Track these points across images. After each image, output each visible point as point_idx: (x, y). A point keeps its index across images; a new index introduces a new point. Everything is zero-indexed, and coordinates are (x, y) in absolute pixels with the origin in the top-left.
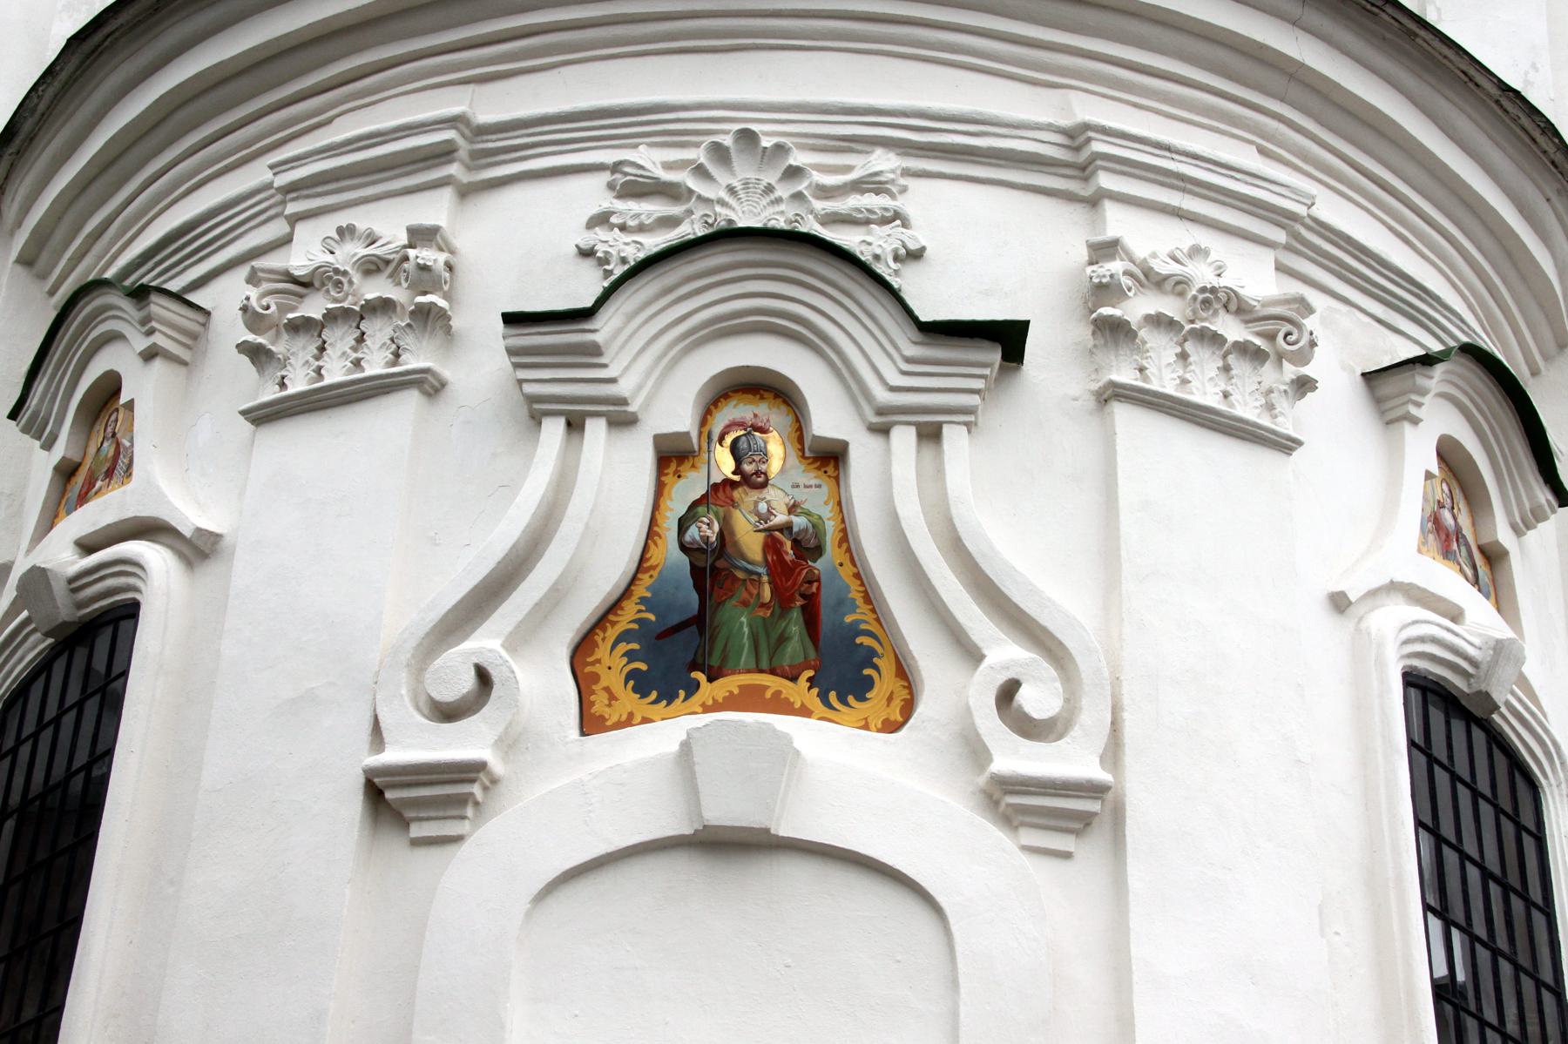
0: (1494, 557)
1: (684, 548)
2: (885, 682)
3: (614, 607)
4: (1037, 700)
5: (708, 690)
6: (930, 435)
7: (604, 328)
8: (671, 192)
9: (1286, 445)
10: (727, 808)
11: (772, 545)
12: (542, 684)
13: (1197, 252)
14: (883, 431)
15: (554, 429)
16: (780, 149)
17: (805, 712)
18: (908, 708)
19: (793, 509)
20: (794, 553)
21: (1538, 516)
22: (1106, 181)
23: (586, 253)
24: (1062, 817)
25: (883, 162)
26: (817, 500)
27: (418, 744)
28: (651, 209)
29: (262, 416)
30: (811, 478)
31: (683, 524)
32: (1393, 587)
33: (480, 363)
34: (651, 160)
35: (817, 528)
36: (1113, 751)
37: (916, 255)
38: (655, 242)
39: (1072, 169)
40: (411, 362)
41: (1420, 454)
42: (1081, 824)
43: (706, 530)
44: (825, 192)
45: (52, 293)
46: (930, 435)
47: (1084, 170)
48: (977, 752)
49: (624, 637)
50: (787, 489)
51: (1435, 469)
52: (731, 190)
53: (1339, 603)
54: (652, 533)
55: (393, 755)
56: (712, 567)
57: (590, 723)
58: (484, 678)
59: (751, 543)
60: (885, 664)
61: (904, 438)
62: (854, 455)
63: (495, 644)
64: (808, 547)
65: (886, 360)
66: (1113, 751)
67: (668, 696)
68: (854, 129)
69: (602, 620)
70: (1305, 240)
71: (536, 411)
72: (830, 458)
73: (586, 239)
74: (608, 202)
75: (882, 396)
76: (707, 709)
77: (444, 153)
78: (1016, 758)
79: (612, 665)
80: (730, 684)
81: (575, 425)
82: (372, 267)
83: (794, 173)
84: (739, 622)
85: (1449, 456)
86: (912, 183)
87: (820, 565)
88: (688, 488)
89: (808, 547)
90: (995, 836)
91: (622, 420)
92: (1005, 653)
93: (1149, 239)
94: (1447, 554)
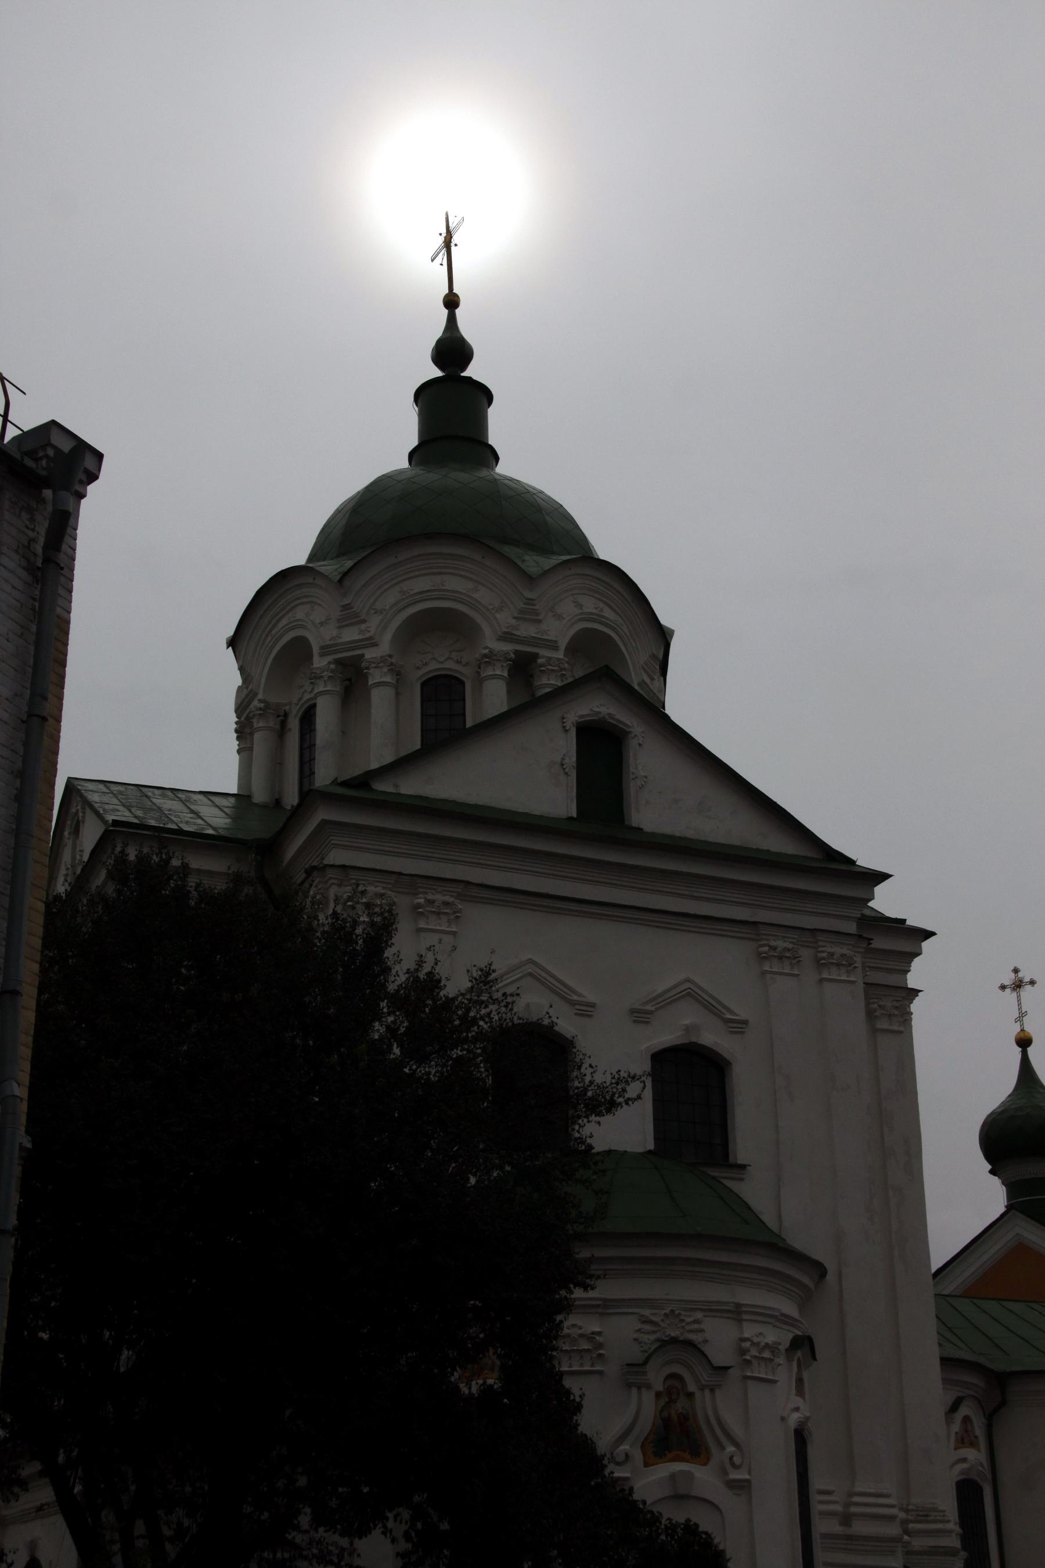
4: (737, 1460)
6: (712, 1391)
8: (651, 1322)
9: (774, 1382)
12: (638, 1455)
15: (634, 1391)
16: (680, 1314)
17: (688, 1461)
18: (708, 1459)
23: (635, 1340)
24: (741, 1487)
25: (699, 1315)
28: (648, 1327)
34: (647, 1312)
39: (737, 1313)
40: (597, 1368)
46: (712, 1391)
53: (783, 1419)
57: (646, 1465)
58: (627, 1456)
61: (707, 1392)
69: (646, 1438)
71: (629, 1385)
72: (690, 1395)
73: (636, 1336)
74: (639, 1326)
75: (704, 1383)
77: (598, 1306)
78: (734, 1475)
81: (639, 1388)
82: (582, 1336)
83: (682, 1321)
88: (662, 1402)
91: (649, 1387)
92: (731, 1449)
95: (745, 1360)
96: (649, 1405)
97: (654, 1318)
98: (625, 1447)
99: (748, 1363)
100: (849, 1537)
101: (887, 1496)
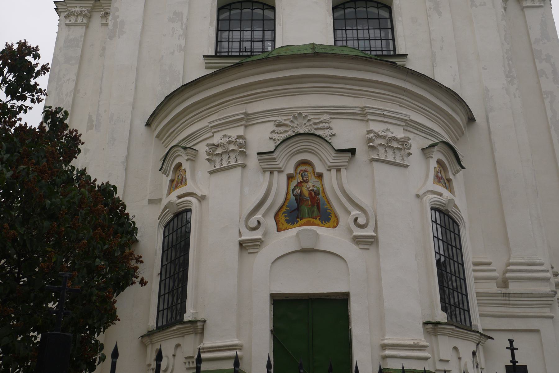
0: (449, 181)
1: (294, 195)
2: (333, 219)
3: (281, 207)
4: (361, 221)
5: (300, 222)
6: (338, 170)
7: (275, 155)
9: (406, 166)
10: (307, 245)
11: (310, 194)
12: (270, 222)
13: (388, 130)
14: (329, 170)
15: (268, 174)
17: (318, 225)
18: (337, 223)
19: (313, 186)
20: (315, 195)
21: (458, 171)
22: (369, 117)
23: (271, 138)
24: (368, 242)
25: (326, 117)
26: (318, 185)
27: (248, 235)
29: (211, 173)
30: (317, 180)
31: (293, 191)
32: (428, 191)
33: (253, 161)
34: (281, 119)
35: (318, 190)
36: (376, 230)
37: (334, 135)
38: (284, 136)
39: (362, 115)
40: (240, 162)
41: (433, 164)
42: (371, 243)
43: (298, 191)
44: (315, 124)
45: (163, 143)
46: (338, 170)
47: (365, 115)
48: (351, 231)
49: (284, 213)
50: (312, 183)
51: (436, 166)
52: (298, 125)
53: (418, 196)
54: (287, 192)
55: (243, 238)
56: (299, 198)
57: (279, 230)
59: (306, 194)
60: (333, 215)
61: (334, 172)
62: (324, 175)
63: (260, 216)
64: (317, 193)
65: (330, 157)
66: (376, 230)
67: (293, 224)
68: (320, 111)
69: (280, 210)
70: (409, 124)
72: (320, 176)
73: (271, 136)
74: (274, 128)
75: (329, 164)
76: (300, 226)
79: (282, 218)
80: (304, 221)
81: (271, 173)
82: (230, 143)
84: (305, 209)
85: (439, 162)
86: (333, 121)
87: (319, 197)
88: (294, 183)
89: (317, 193)
90: (355, 247)
91: (280, 171)
92: (355, 212)
93: (378, 128)
94: (439, 182)
95: (370, 146)
96: (280, 184)
97: (288, 122)
98: (258, 216)
99: (373, 147)
100: (507, 295)
101: (542, 264)
